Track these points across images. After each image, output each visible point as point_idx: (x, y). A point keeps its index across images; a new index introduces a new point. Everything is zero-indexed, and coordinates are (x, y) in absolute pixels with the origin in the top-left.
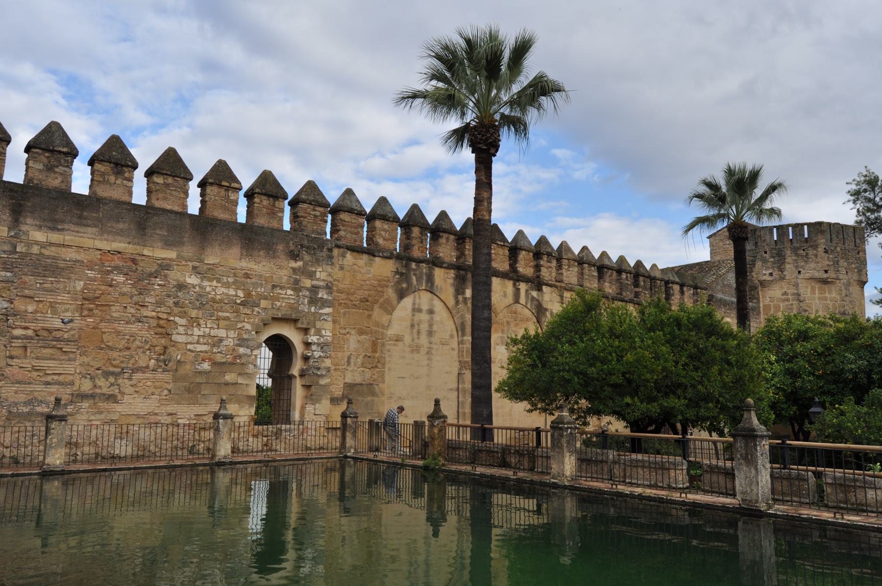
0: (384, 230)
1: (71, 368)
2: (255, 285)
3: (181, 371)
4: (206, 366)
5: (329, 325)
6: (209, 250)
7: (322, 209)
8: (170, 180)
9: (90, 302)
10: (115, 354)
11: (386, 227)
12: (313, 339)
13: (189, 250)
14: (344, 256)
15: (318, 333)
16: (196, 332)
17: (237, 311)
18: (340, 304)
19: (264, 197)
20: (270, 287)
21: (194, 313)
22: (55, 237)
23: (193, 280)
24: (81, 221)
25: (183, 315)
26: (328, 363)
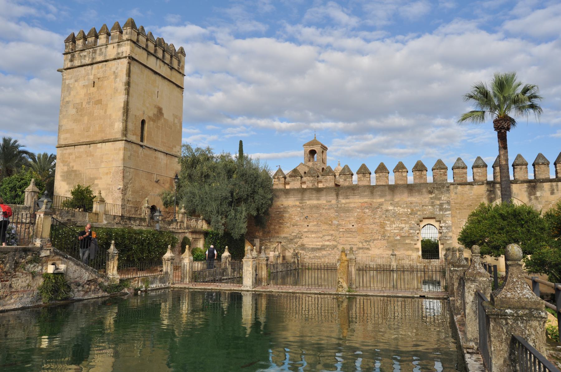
0: (479, 172)
1: (356, 240)
2: (415, 206)
3: (390, 240)
4: (398, 238)
5: (450, 219)
6: (395, 197)
7: (444, 170)
8: (381, 174)
9: (360, 219)
10: (368, 235)
11: (479, 171)
12: (443, 225)
13: (388, 197)
14: (456, 188)
15: (445, 222)
16: (394, 226)
17: (408, 217)
18: (457, 209)
19: (417, 172)
20: (421, 206)
21: (392, 219)
22: (348, 201)
23: (391, 208)
24: (354, 195)
25: (389, 220)
26: (450, 234)
